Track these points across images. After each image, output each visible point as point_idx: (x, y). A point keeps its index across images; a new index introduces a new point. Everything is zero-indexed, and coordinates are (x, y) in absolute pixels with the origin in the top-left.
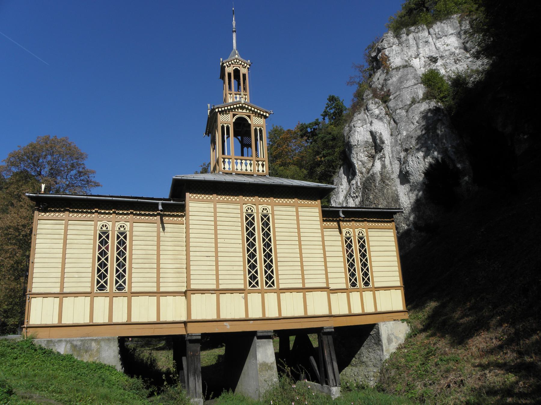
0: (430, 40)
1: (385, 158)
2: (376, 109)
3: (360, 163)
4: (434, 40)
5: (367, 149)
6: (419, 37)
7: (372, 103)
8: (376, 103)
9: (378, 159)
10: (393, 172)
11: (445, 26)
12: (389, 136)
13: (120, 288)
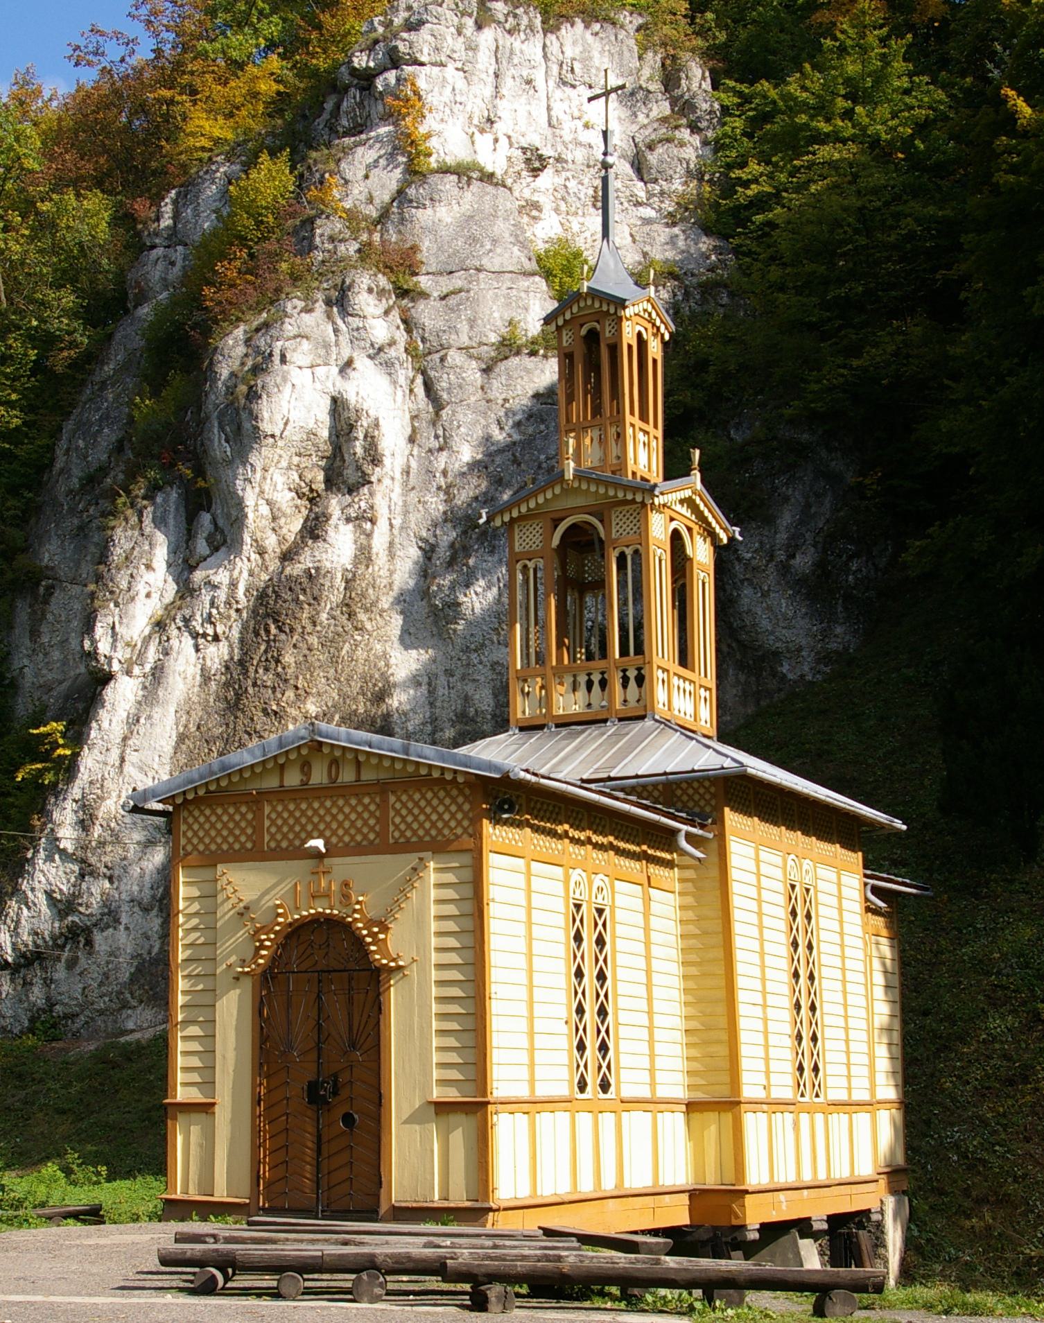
0: (540, 82)
1: (373, 521)
2: (376, 317)
3: (265, 510)
4: (551, 83)
5: (305, 462)
6: (512, 52)
9: (348, 520)
11: (595, 45)
12: (402, 442)
13: (605, 1086)
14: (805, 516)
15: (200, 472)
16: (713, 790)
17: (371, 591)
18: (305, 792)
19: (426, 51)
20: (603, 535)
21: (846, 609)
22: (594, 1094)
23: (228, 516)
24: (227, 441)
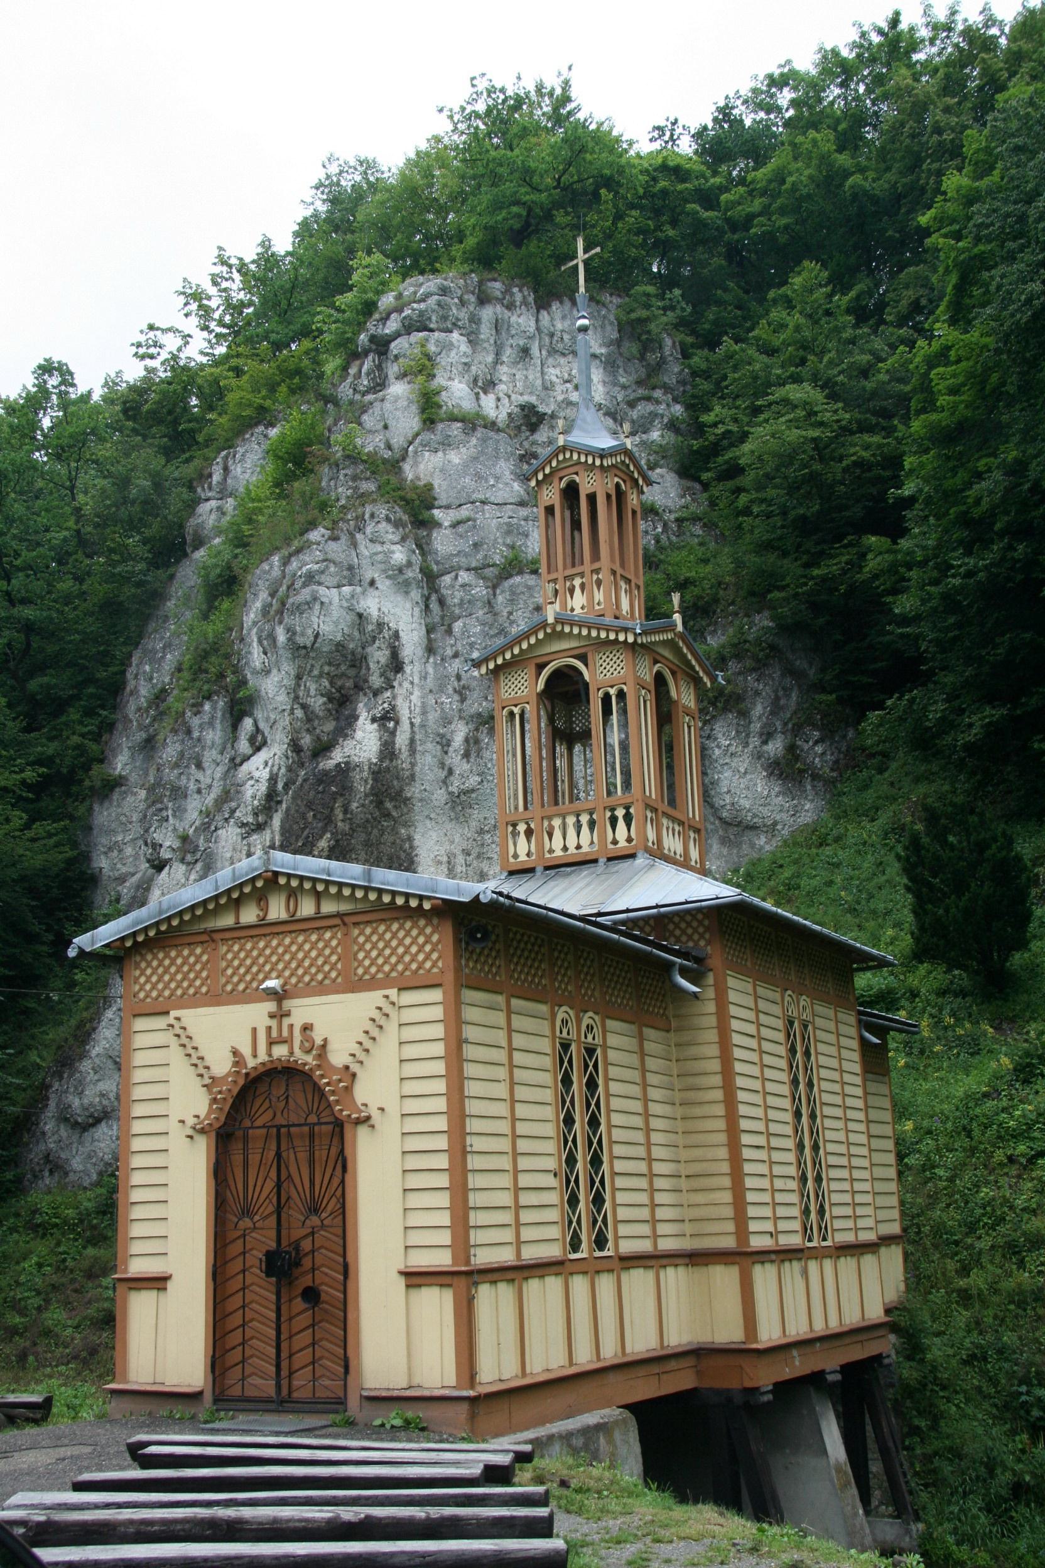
0: (535, 351)
1: (397, 723)
3: (299, 713)
4: (544, 353)
7: (388, 519)
8: (398, 524)
9: (374, 720)
10: (412, 777)
12: (420, 652)
14: (776, 708)
15: (243, 683)
16: (706, 922)
17: (395, 783)
18: (265, 928)
19: (434, 318)
20: (587, 677)
21: (814, 787)
22: (591, 1251)
23: (267, 719)
24: (265, 653)
